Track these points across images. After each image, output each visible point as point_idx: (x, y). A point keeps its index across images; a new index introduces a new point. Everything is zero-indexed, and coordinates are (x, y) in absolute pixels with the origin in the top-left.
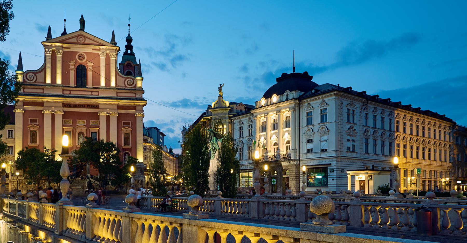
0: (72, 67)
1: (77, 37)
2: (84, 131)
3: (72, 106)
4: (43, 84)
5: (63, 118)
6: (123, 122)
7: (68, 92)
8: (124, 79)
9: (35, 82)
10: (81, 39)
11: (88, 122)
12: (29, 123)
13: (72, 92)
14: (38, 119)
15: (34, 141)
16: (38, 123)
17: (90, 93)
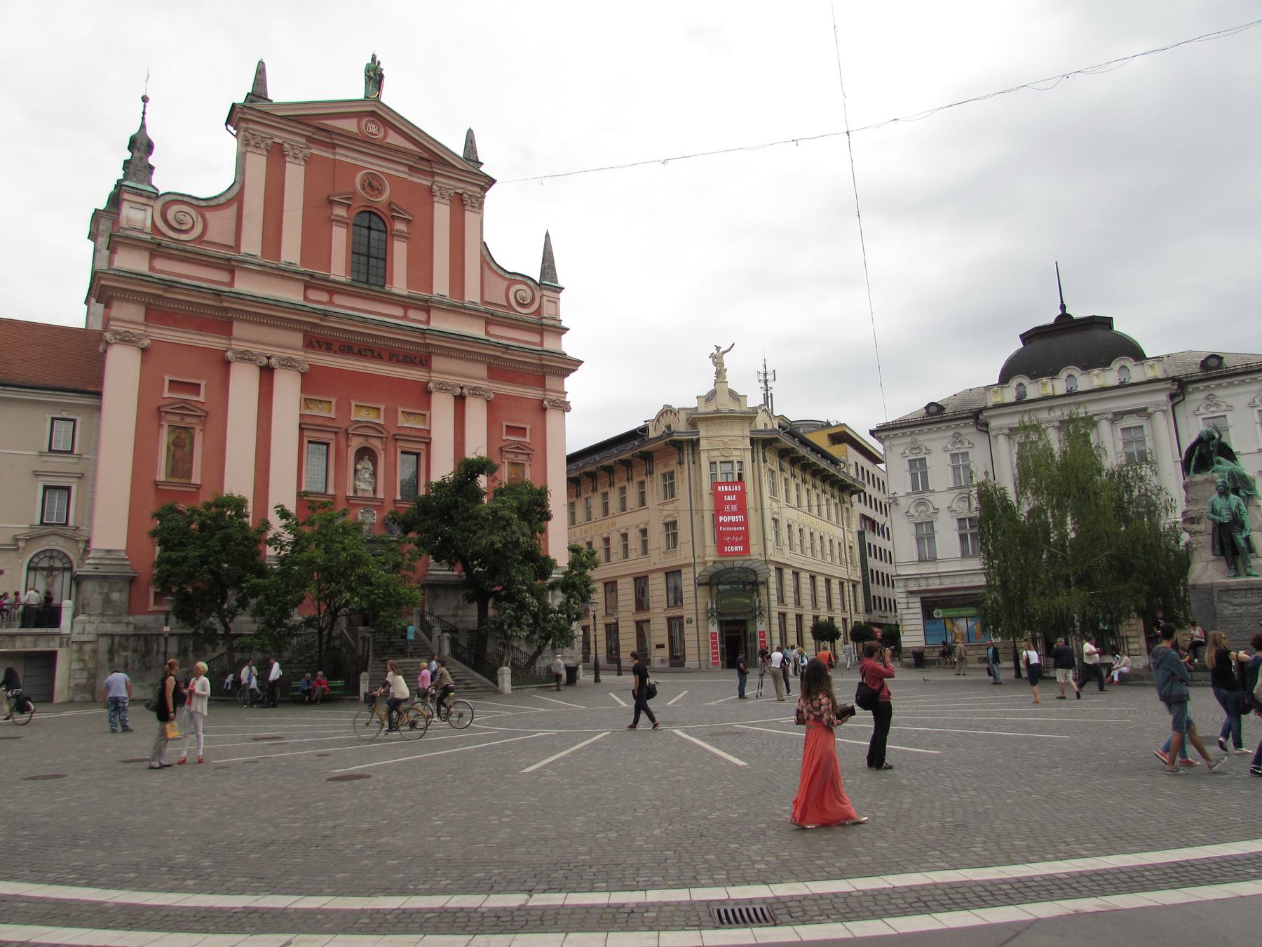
0: (340, 211)
1: (359, 115)
2: (376, 444)
3: (335, 347)
4: (229, 254)
5: (303, 390)
6: (505, 424)
7: (324, 297)
8: (505, 284)
9: (199, 240)
10: (373, 128)
11: (391, 414)
12: (166, 394)
13: (338, 299)
14: (203, 383)
16: (201, 399)
17: (399, 312)
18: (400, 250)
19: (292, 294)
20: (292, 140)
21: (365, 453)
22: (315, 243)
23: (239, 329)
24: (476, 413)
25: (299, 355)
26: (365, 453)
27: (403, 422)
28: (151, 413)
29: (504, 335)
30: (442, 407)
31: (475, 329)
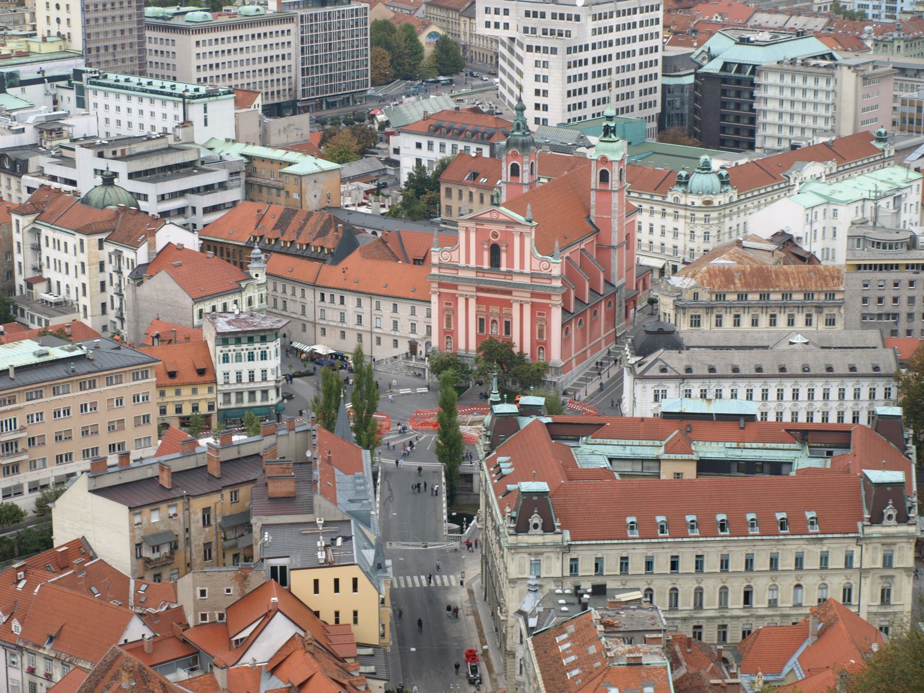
0: (486, 246)
2: (497, 319)
11: (501, 310)
15: (449, 325)
18: (504, 256)
19: (472, 275)
20: (471, 225)
21: (494, 321)
22: (479, 259)
23: (459, 288)
24: (527, 309)
25: (474, 294)
26: (494, 321)
27: (504, 311)
28: (441, 311)
29: (538, 282)
30: (516, 308)
31: (527, 280)
